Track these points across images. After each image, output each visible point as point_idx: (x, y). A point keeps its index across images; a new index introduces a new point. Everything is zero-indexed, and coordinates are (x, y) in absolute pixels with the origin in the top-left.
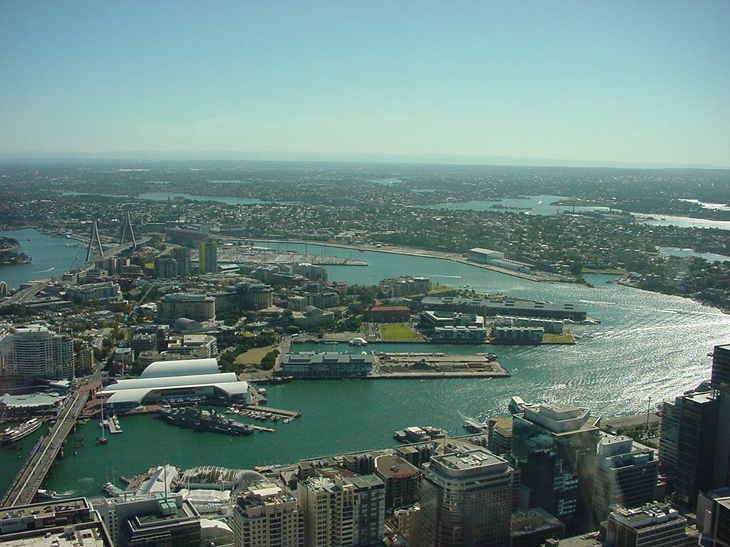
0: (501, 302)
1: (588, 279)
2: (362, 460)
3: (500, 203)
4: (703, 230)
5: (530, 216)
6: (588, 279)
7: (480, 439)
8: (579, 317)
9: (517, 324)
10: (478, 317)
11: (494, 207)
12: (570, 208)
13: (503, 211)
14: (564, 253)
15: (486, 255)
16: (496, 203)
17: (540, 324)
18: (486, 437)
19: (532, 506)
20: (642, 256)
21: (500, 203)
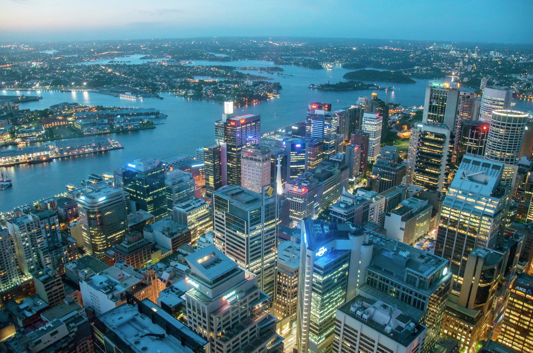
1: (161, 94)
5: (129, 66)
6: (161, 94)
8: (157, 115)
10: (104, 120)
11: (111, 62)
12: (150, 60)
13: (115, 64)
16: (112, 60)
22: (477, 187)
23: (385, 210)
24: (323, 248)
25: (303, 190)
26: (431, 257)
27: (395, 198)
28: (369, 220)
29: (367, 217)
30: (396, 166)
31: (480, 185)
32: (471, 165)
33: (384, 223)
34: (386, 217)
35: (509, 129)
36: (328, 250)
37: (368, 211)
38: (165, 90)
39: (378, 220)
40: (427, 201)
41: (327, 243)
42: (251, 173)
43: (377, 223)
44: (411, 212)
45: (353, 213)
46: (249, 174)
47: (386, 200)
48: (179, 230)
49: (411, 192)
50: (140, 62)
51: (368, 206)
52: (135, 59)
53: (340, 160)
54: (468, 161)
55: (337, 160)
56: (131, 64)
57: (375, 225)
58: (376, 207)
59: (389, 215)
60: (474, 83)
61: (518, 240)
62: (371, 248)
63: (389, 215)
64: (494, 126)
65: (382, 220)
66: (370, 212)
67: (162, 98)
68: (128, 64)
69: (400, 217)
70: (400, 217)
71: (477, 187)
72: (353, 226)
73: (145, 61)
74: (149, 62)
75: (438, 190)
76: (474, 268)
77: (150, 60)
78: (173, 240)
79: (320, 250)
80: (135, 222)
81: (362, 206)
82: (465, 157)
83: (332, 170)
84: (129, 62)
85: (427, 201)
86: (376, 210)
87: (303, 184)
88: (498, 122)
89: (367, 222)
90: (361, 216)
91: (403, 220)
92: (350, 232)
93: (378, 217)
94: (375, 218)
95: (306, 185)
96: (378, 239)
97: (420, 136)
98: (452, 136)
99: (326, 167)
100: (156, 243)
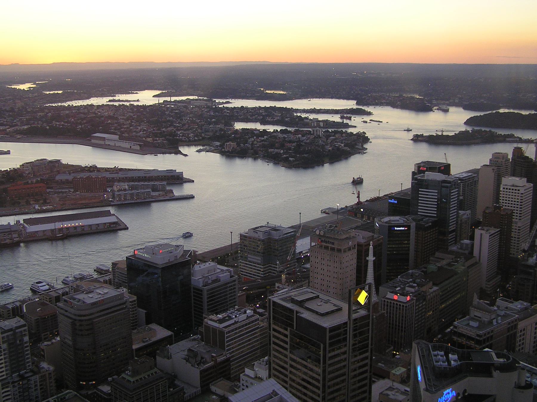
0: (118, 173)
2: (13, 309)
3: (114, 98)
4: (265, 108)
6: (184, 150)
7: (107, 278)
9: (132, 188)
11: (110, 101)
12: (168, 99)
13: (116, 104)
14: (164, 132)
15: (105, 138)
16: (111, 98)
17: (147, 187)
18: (111, 277)
19: (149, 321)
20: (221, 130)
21: (114, 98)
24: (448, 390)
25: (408, 298)
28: (517, 349)
36: (458, 394)
37: (515, 334)
38: (189, 143)
41: (455, 382)
42: (326, 270)
43: (531, 352)
45: (492, 336)
46: (322, 272)
48: (213, 357)
50: (156, 101)
51: (516, 326)
52: (147, 98)
53: (467, 252)
56: (140, 104)
66: (518, 335)
67: (186, 155)
68: (136, 104)
73: (161, 100)
74: (167, 101)
77: (168, 99)
78: (201, 372)
79: (445, 393)
80: (144, 342)
84: (138, 101)
87: (407, 289)
92: (493, 364)
95: (413, 290)
99: (444, 262)
100: (175, 377)
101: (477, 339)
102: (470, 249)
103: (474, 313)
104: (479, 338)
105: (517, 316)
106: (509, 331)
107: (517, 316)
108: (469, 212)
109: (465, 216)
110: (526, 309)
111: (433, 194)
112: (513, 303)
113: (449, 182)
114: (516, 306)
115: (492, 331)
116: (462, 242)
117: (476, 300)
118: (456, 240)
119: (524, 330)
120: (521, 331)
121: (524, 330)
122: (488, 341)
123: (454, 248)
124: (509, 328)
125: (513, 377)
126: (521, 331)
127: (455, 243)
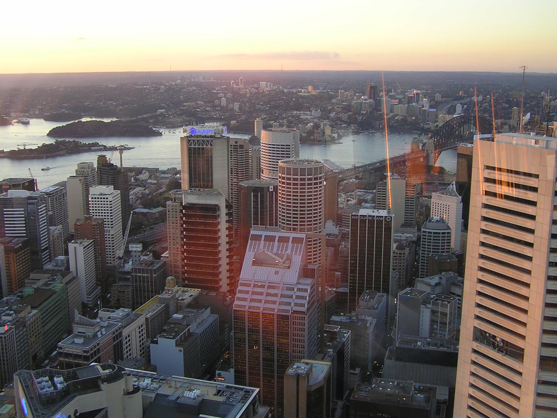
22: (277, 273)
23: (148, 337)
26: (233, 390)
27: (159, 314)
28: (125, 356)
29: (122, 351)
30: (152, 263)
31: (281, 271)
32: (262, 242)
33: (149, 356)
34: (152, 345)
35: (304, 185)
37: (121, 341)
39: (139, 353)
40: (209, 309)
43: (139, 357)
44: (189, 330)
45: (99, 349)
47: (147, 319)
49: (183, 300)
51: (120, 334)
53: (63, 268)
54: (257, 238)
55: (57, 268)
57: (137, 361)
58: (133, 333)
59: (156, 342)
60: (246, 127)
61: (344, 340)
62: (137, 400)
63: (156, 342)
64: (283, 183)
65: (146, 353)
66: (124, 342)
69: (173, 341)
70: (173, 341)
71: (277, 273)
72: (104, 368)
75: (221, 290)
76: (295, 393)
81: (111, 336)
82: (252, 232)
83: (50, 287)
85: (209, 309)
86: (133, 337)
88: (288, 176)
89: (122, 359)
90: (112, 352)
91: (177, 345)
93: (139, 348)
94: (134, 351)
95: (9, 318)
96: (148, 381)
97: (181, 211)
98: (229, 207)
101: (84, 356)
102: (65, 265)
103: (77, 329)
104: (85, 354)
105: (120, 324)
106: (114, 341)
107: (120, 324)
108: (60, 226)
109: (57, 232)
110: (128, 315)
111: (19, 212)
112: (114, 312)
113: (35, 198)
114: (118, 314)
115: (98, 344)
116: (56, 258)
117: (78, 316)
118: (50, 258)
119: (129, 336)
120: (126, 338)
121: (129, 336)
122: (95, 355)
123: (49, 266)
124: (114, 338)
125: (120, 385)
126: (126, 338)
127: (50, 261)
